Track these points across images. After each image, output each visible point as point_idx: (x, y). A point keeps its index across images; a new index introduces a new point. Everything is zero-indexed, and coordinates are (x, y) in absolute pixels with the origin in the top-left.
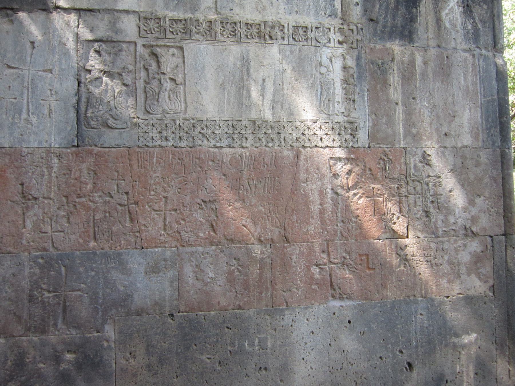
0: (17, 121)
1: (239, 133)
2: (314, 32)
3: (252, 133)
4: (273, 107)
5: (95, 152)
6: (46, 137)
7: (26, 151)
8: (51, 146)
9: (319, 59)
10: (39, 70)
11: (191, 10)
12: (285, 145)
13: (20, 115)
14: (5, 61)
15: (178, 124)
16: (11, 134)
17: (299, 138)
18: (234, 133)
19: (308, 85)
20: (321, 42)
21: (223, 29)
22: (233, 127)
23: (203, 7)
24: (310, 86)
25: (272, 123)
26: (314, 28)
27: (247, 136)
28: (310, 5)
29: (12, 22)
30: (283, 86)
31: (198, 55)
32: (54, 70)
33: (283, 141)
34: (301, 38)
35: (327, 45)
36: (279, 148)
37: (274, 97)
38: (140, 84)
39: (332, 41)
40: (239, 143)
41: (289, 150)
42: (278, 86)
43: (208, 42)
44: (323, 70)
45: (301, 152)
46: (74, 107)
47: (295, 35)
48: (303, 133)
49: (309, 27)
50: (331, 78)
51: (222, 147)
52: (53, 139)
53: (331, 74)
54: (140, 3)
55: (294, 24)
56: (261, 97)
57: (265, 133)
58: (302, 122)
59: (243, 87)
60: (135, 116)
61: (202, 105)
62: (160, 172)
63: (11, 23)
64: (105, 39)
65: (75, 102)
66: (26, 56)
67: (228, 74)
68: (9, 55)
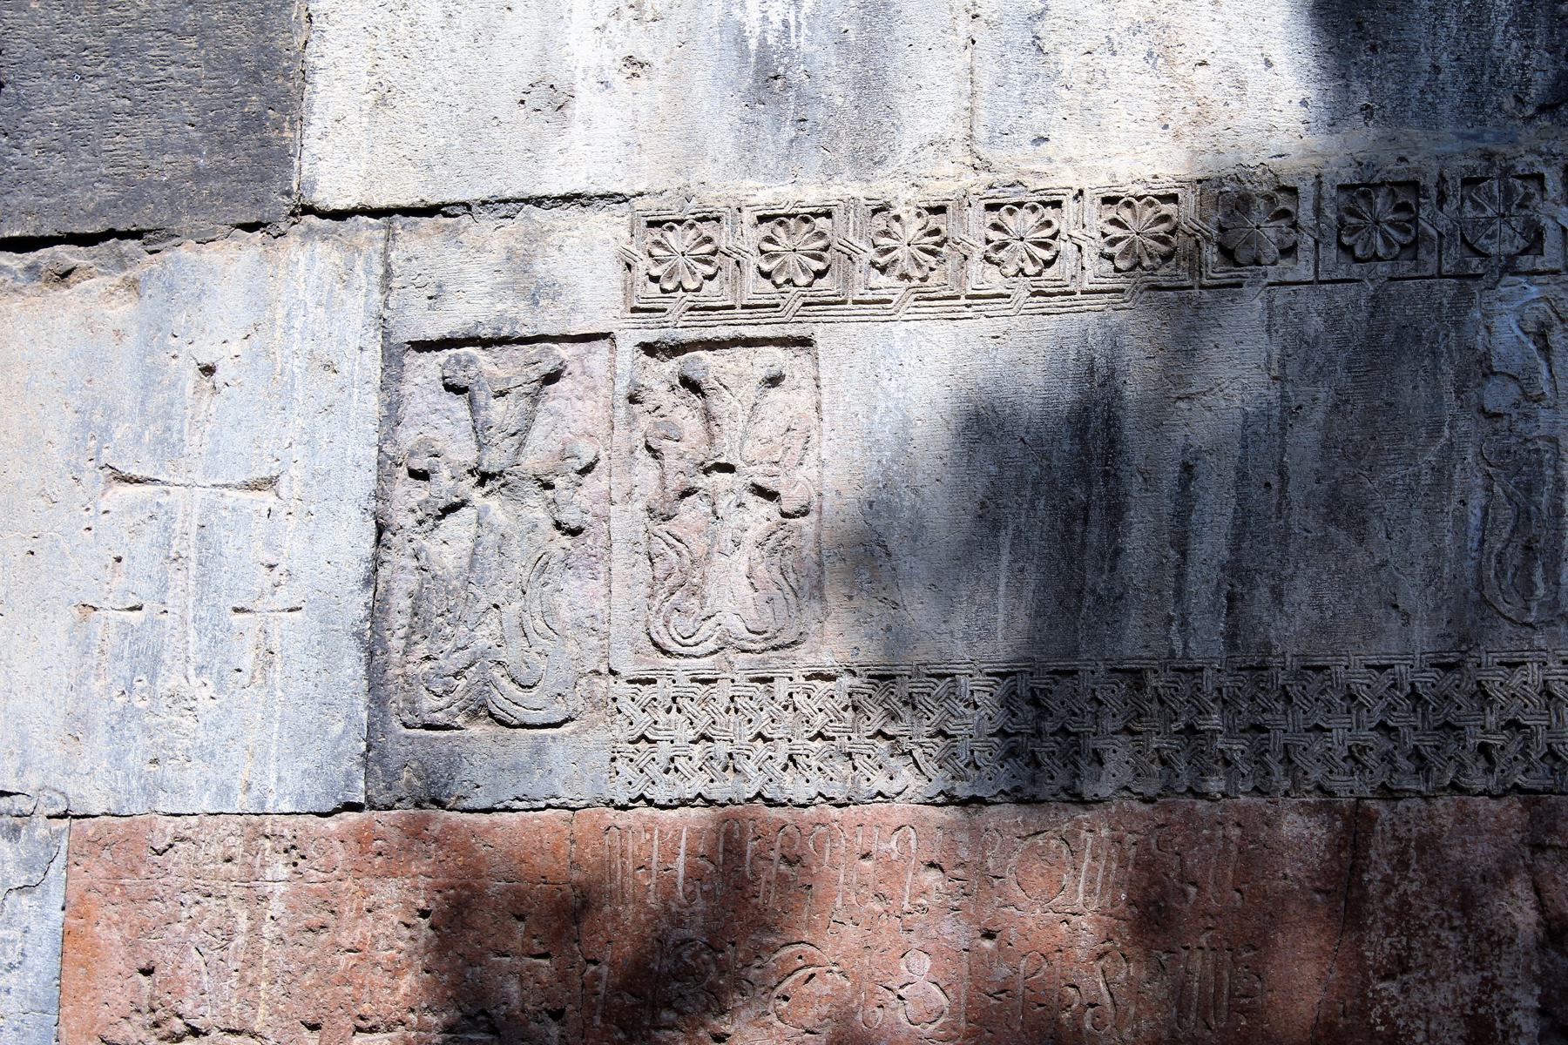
0: (141, 705)
1: (1063, 731)
2: (1451, 206)
3: (1128, 730)
4: (1231, 598)
5: (435, 829)
6: (246, 771)
7: (170, 830)
8: (262, 804)
9: (1479, 341)
10: (226, 486)
11: (854, 159)
12: (1287, 784)
13: (153, 677)
14: (106, 456)
15: (782, 696)
16: (118, 758)
17: (1363, 750)
18: (1039, 733)
19: (1417, 476)
20: (1493, 250)
21: (997, 237)
22: (1035, 702)
23: (908, 140)
24: (1426, 479)
25: (1227, 682)
26: (1454, 185)
27: (1100, 745)
28: (1436, 69)
29: (132, 285)
30: (1283, 490)
31: (881, 370)
32: (284, 479)
33: (1278, 770)
34: (1388, 242)
35: (1526, 262)
36: (1260, 801)
37: (1235, 548)
38: (626, 521)
39: (1552, 240)
40: (1062, 778)
41: (1315, 810)
42: (1257, 494)
43: (926, 308)
44: (1497, 396)
45: (1370, 818)
46: (359, 635)
47: (1356, 229)
48: (1382, 725)
49: (1429, 182)
50: (1543, 431)
51: (981, 801)
52: (273, 777)
53: (1543, 413)
54: (636, 159)
55: (1347, 176)
56: (1173, 554)
57: (1190, 730)
58: (1381, 668)
59: (1086, 509)
60: (603, 669)
61: (895, 606)
62: (700, 919)
63: (133, 294)
64: (485, 332)
65: (364, 613)
66: (181, 431)
67: (1016, 451)
68: (120, 431)
